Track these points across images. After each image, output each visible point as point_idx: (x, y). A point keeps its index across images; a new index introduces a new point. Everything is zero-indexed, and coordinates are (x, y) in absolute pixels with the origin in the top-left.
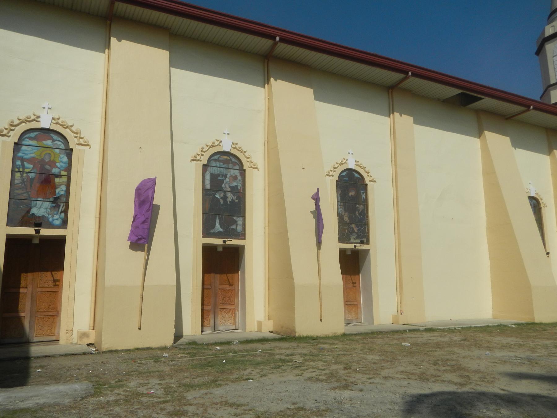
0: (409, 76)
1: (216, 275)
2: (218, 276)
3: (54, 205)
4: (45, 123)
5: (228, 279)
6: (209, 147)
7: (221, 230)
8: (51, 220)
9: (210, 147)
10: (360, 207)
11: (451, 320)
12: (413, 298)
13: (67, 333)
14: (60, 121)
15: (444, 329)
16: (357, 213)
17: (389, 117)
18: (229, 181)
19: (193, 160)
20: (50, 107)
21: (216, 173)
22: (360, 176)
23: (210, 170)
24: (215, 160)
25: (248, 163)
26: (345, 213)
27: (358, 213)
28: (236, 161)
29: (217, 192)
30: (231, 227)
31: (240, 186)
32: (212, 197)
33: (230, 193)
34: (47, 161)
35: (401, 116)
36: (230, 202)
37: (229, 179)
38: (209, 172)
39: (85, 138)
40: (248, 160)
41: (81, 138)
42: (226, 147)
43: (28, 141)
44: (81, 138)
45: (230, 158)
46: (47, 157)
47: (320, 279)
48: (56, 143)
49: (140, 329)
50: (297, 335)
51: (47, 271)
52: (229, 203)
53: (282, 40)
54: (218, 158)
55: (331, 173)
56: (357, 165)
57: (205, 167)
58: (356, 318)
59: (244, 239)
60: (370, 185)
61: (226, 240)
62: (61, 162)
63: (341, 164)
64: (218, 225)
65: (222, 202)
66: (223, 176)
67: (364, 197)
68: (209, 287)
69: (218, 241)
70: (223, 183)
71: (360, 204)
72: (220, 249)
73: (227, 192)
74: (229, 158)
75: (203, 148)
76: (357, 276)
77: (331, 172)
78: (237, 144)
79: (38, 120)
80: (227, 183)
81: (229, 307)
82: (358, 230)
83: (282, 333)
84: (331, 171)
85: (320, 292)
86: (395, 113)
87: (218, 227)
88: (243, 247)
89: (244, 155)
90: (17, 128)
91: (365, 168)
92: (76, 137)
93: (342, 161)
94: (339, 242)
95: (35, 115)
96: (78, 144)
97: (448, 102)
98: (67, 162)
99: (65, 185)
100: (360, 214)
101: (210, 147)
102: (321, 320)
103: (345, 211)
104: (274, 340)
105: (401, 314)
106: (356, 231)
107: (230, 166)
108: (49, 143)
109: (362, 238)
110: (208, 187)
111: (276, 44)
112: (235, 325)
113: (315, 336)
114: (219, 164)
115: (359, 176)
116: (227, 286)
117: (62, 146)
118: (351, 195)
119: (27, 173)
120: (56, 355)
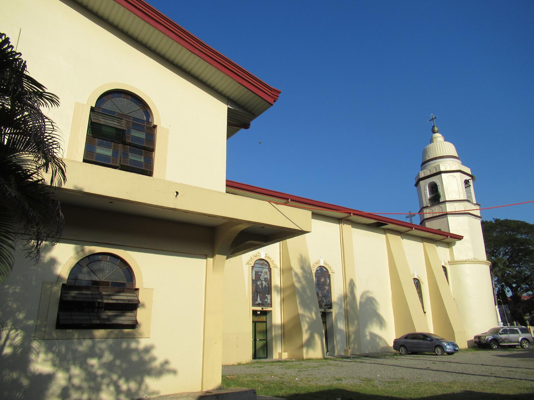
21: (257, 271)
28: (267, 264)
30: (265, 300)
32: (256, 284)
37: (264, 274)
59: (272, 307)
64: (259, 299)
87: (259, 301)
88: (271, 311)
100: (327, 292)
107: (264, 266)
110: (254, 278)
118: (322, 281)
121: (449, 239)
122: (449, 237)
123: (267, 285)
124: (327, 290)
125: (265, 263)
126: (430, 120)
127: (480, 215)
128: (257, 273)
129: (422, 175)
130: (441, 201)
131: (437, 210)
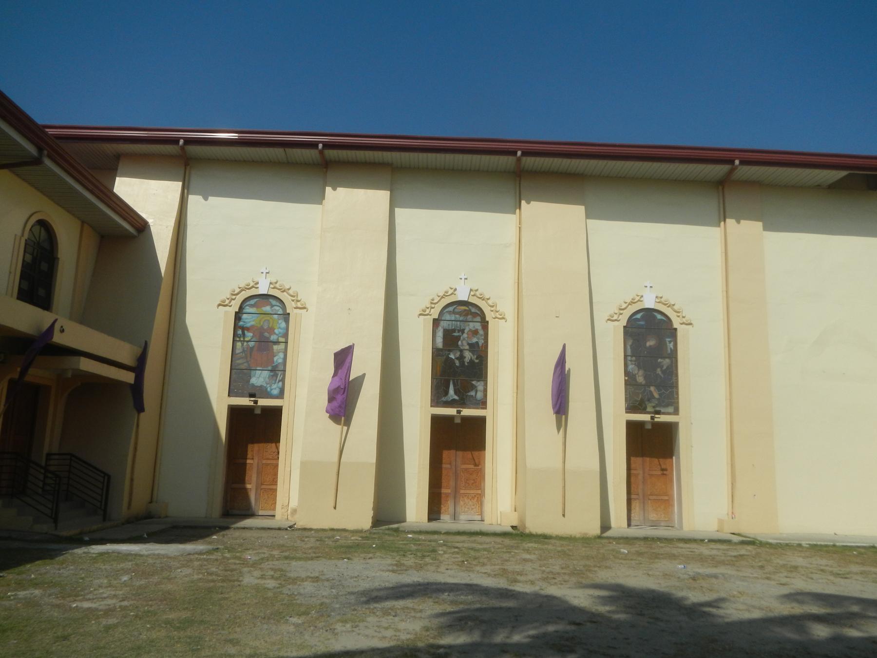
0: (737, 166)
2: (460, 453)
3: (272, 374)
4: (263, 290)
5: (473, 456)
7: (456, 397)
8: (269, 389)
9: (442, 297)
10: (665, 362)
11: (835, 534)
12: (755, 495)
13: (282, 508)
14: (277, 285)
15: (777, 543)
16: (659, 371)
18: (467, 337)
19: (420, 315)
20: (268, 271)
21: (450, 328)
22: (665, 318)
24: (450, 312)
26: (639, 371)
27: (661, 371)
29: (451, 351)
30: (469, 394)
31: (481, 342)
33: (468, 351)
34: (265, 327)
35: (738, 222)
36: (468, 363)
37: (467, 334)
39: (302, 300)
40: (492, 309)
42: (462, 296)
43: (248, 309)
50: (527, 531)
51: (272, 443)
52: (466, 364)
57: (436, 322)
58: (666, 519)
59: (486, 408)
62: (280, 328)
63: (633, 302)
64: (451, 391)
65: (457, 363)
66: (459, 331)
67: (672, 347)
68: (448, 466)
69: (451, 411)
70: (459, 339)
71: (664, 358)
74: (467, 308)
75: (433, 300)
78: (477, 290)
80: (464, 339)
81: (472, 492)
82: (660, 395)
86: (727, 220)
89: (487, 302)
90: (238, 297)
92: (293, 301)
95: (254, 282)
96: (295, 308)
97: (834, 188)
100: (664, 372)
103: (639, 367)
105: (732, 518)
106: (656, 395)
107: (469, 318)
108: (267, 309)
114: (455, 317)
115: (663, 318)
116: (472, 466)
117: (281, 312)
118: (650, 346)
119: (248, 341)
120: (253, 527)
123: (477, 359)
124: (665, 367)
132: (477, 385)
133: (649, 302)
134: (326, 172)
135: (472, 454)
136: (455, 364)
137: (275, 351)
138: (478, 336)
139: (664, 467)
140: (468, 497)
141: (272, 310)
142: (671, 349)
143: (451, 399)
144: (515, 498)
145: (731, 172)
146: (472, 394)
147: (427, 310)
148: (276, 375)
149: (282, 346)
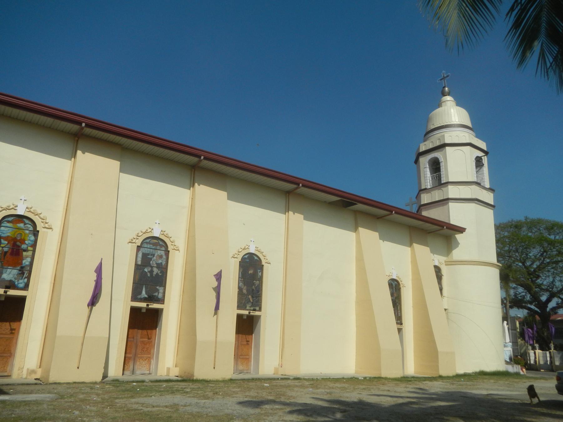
0: (300, 187)
1: (139, 331)
2: (140, 331)
3: (20, 272)
4: (21, 211)
6: (143, 233)
8: (16, 283)
9: (144, 233)
11: (321, 373)
13: (19, 370)
14: (32, 210)
15: (308, 378)
17: (285, 214)
18: (156, 259)
19: (129, 242)
20: (26, 199)
23: (142, 250)
24: (147, 243)
25: (172, 246)
26: (244, 286)
27: (254, 287)
29: (145, 267)
31: (164, 263)
32: (141, 271)
33: (156, 268)
34: (19, 239)
35: (294, 214)
36: (155, 275)
37: (156, 257)
38: (141, 252)
40: (173, 244)
41: (46, 223)
42: (156, 234)
43: (6, 224)
44: (46, 223)
45: (159, 242)
46: (19, 236)
47: (216, 337)
48: (27, 226)
49: (78, 368)
50: (195, 378)
51: (6, 322)
52: (154, 276)
53: (205, 158)
54: (150, 241)
55: (236, 256)
56: (257, 250)
59: (163, 304)
60: (266, 266)
61: (149, 304)
62: (29, 240)
63: (244, 249)
64: (144, 292)
65: (149, 275)
67: (260, 275)
68: (132, 339)
69: (143, 305)
70: (151, 260)
71: (256, 280)
72: (144, 311)
73: (154, 268)
74: (157, 242)
75: (138, 234)
76: (251, 336)
77: (236, 255)
78: (165, 231)
79: (16, 208)
80: (154, 260)
81: (145, 356)
83: (184, 377)
84: (236, 254)
85: (216, 347)
87: (144, 294)
88: (162, 310)
89: (169, 239)
91: (263, 252)
92: (43, 222)
93: (245, 247)
94: (237, 309)
95: (13, 205)
96: (44, 228)
97: (332, 204)
98: (34, 241)
99: (30, 257)
101: (144, 233)
102: (214, 368)
104: (177, 381)
105: (281, 367)
106: (251, 301)
107: (158, 247)
108: (21, 225)
109: (255, 307)
110: (139, 263)
111: (201, 161)
112: (150, 370)
113: (209, 380)
114: (150, 246)
115: (258, 259)
116: (146, 340)
117: (31, 229)
118: (250, 273)
120: (16, 384)
121: (446, 231)
122: (445, 227)
123: (160, 273)
124: (257, 285)
125: (161, 243)
126: (441, 80)
127: (494, 203)
128: (145, 256)
129: (423, 148)
130: (442, 182)
131: (437, 195)
132: (159, 289)
133: (252, 250)
134: (78, 141)
135: (147, 332)
136: (147, 275)
137: (24, 256)
138: (162, 259)
139: (248, 340)
140: (142, 359)
141: (25, 227)
142: (260, 275)
143: (143, 297)
144: (176, 359)
145: (296, 189)
146: (156, 295)
147: (134, 240)
148: (23, 273)
149: (30, 253)
